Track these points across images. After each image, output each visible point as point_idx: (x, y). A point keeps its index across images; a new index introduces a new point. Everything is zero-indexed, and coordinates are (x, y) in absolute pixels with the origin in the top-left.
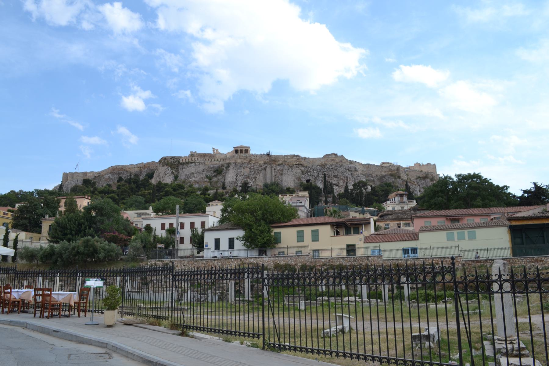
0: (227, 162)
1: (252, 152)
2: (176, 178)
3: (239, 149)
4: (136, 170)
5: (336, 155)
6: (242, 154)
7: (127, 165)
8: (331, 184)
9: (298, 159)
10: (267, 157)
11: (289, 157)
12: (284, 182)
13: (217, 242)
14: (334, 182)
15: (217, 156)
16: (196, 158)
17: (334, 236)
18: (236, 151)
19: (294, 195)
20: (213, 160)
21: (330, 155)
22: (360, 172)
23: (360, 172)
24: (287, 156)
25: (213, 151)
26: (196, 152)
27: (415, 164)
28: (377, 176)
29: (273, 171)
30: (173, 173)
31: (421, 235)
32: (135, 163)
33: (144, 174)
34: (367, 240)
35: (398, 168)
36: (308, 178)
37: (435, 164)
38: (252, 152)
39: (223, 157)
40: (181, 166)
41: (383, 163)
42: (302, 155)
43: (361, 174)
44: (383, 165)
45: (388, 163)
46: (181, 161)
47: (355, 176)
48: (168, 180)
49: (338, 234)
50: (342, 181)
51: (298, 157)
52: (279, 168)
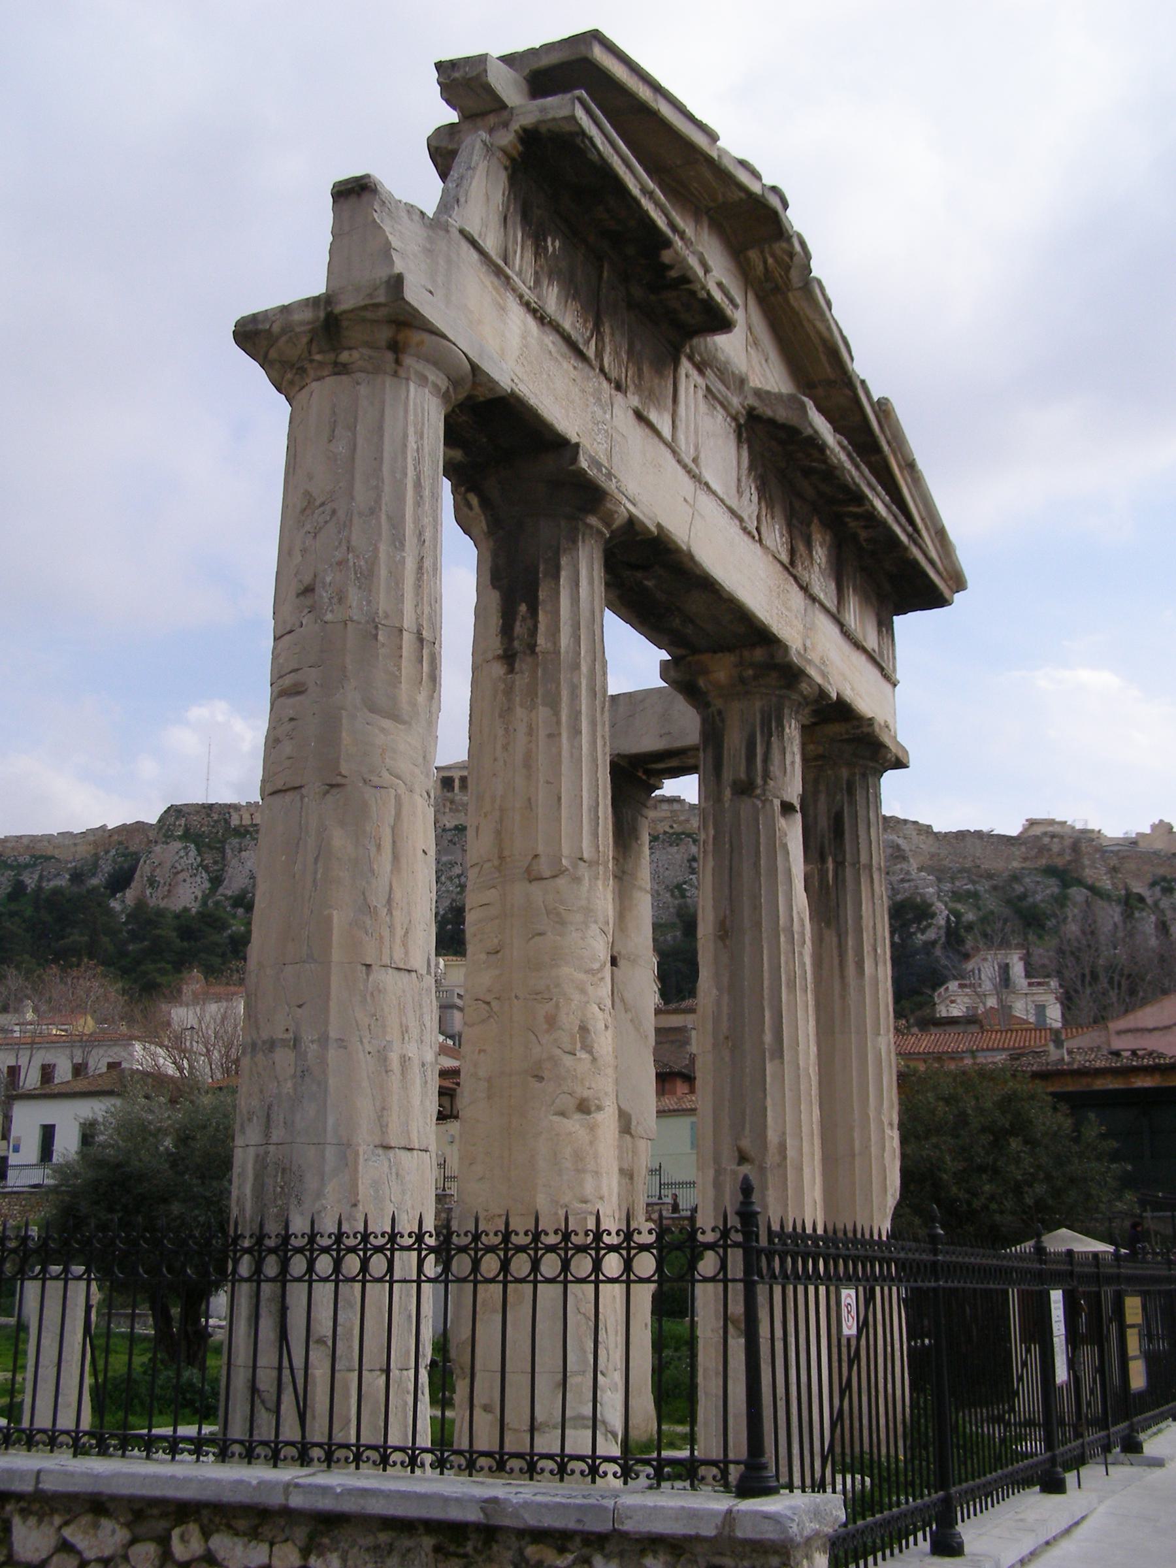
2: (216, 881)
3: (456, 775)
4: (84, 851)
7: (49, 838)
13: (48, 1133)
22: (914, 864)
23: (914, 864)
27: (1154, 827)
28: (990, 876)
30: (206, 868)
32: (78, 827)
33: (106, 867)
35: (1082, 843)
40: (235, 841)
41: (1032, 823)
43: (920, 869)
45: (1052, 822)
46: (235, 822)
47: (895, 879)
51: (676, 806)
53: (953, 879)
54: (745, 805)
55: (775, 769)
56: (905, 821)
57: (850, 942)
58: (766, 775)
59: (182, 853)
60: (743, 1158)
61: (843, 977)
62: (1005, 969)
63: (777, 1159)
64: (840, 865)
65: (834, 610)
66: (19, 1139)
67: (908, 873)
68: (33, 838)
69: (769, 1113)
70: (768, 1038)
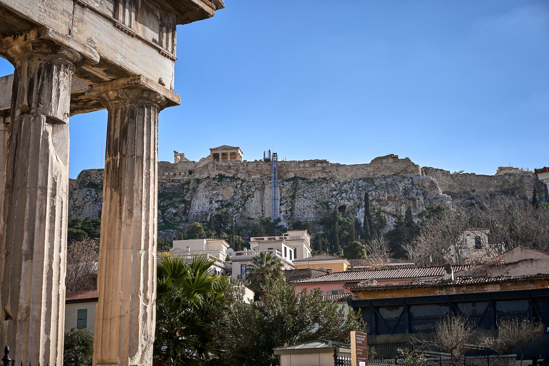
0: (197, 176)
3: (220, 152)
5: (397, 157)
9: (324, 168)
10: (266, 166)
11: (307, 165)
18: (216, 156)
24: (304, 162)
36: (342, 202)
39: (190, 167)
41: (501, 169)
42: (332, 161)
44: (500, 174)
45: (511, 168)
51: (324, 165)
54: (25, 117)
55: (44, 98)
56: (437, 170)
57: (125, 199)
58: (39, 101)
59: (88, 193)
60: (8, 317)
61: (121, 218)
63: (24, 316)
64: (123, 156)
65: (110, 15)
69: (22, 290)
70: (25, 247)
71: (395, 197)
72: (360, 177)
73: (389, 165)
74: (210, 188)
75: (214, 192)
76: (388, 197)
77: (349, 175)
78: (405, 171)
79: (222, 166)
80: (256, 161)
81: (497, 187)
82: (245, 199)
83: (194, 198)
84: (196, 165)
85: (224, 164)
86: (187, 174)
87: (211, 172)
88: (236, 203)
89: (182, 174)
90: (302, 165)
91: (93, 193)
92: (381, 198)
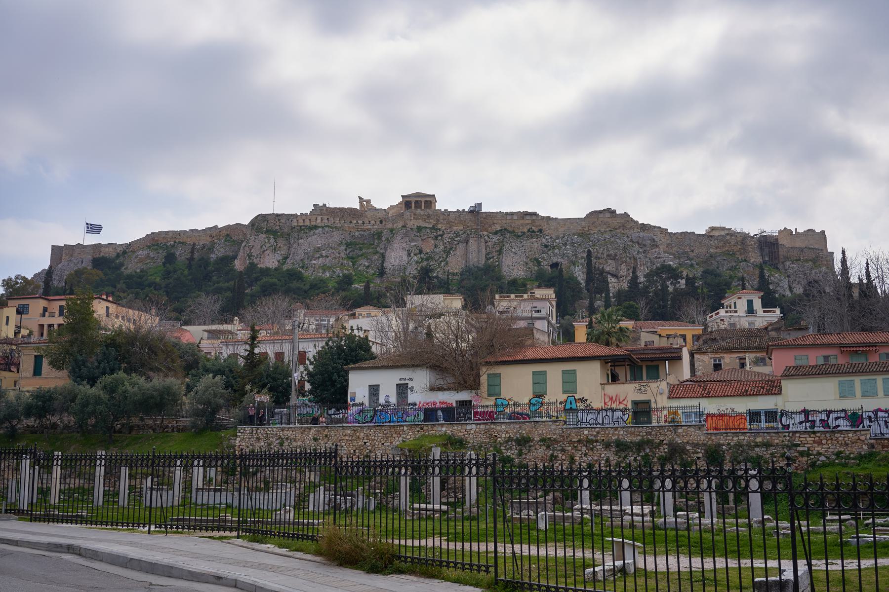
0: (390, 226)
1: (440, 206)
3: (413, 200)
4: (206, 240)
5: (614, 211)
6: (418, 211)
8: (602, 272)
11: (515, 217)
12: (504, 269)
14: (607, 269)
15: (369, 214)
16: (325, 217)
17: (608, 383)
19: (525, 296)
20: (360, 222)
21: (601, 212)
24: (512, 214)
25: (361, 203)
26: (325, 205)
29: (483, 245)
31: (784, 383)
34: (674, 393)
36: (555, 259)
37: (823, 232)
38: (440, 206)
39: (381, 215)
41: (713, 229)
42: (543, 213)
45: (723, 229)
46: (295, 224)
48: (270, 261)
49: (614, 379)
50: (623, 267)
51: (534, 218)
52: (495, 239)
53: (679, 258)
56: (655, 227)
62: (750, 303)
66: (355, 393)
67: (659, 254)
68: (179, 233)
71: (616, 255)
72: (574, 231)
73: (606, 220)
74: (408, 239)
75: (413, 244)
76: (608, 255)
77: (561, 230)
78: (623, 226)
79: (421, 215)
80: (458, 211)
81: (717, 247)
82: (447, 252)
83: (389, 250)
84: (387, 214)
85: (422, 212)
86: (378, 222)
87: (408, 222)
88: (437, 257)
89: (373, 222)
90: (509, 217)
91: (272, 240)
92: (599, 255)
